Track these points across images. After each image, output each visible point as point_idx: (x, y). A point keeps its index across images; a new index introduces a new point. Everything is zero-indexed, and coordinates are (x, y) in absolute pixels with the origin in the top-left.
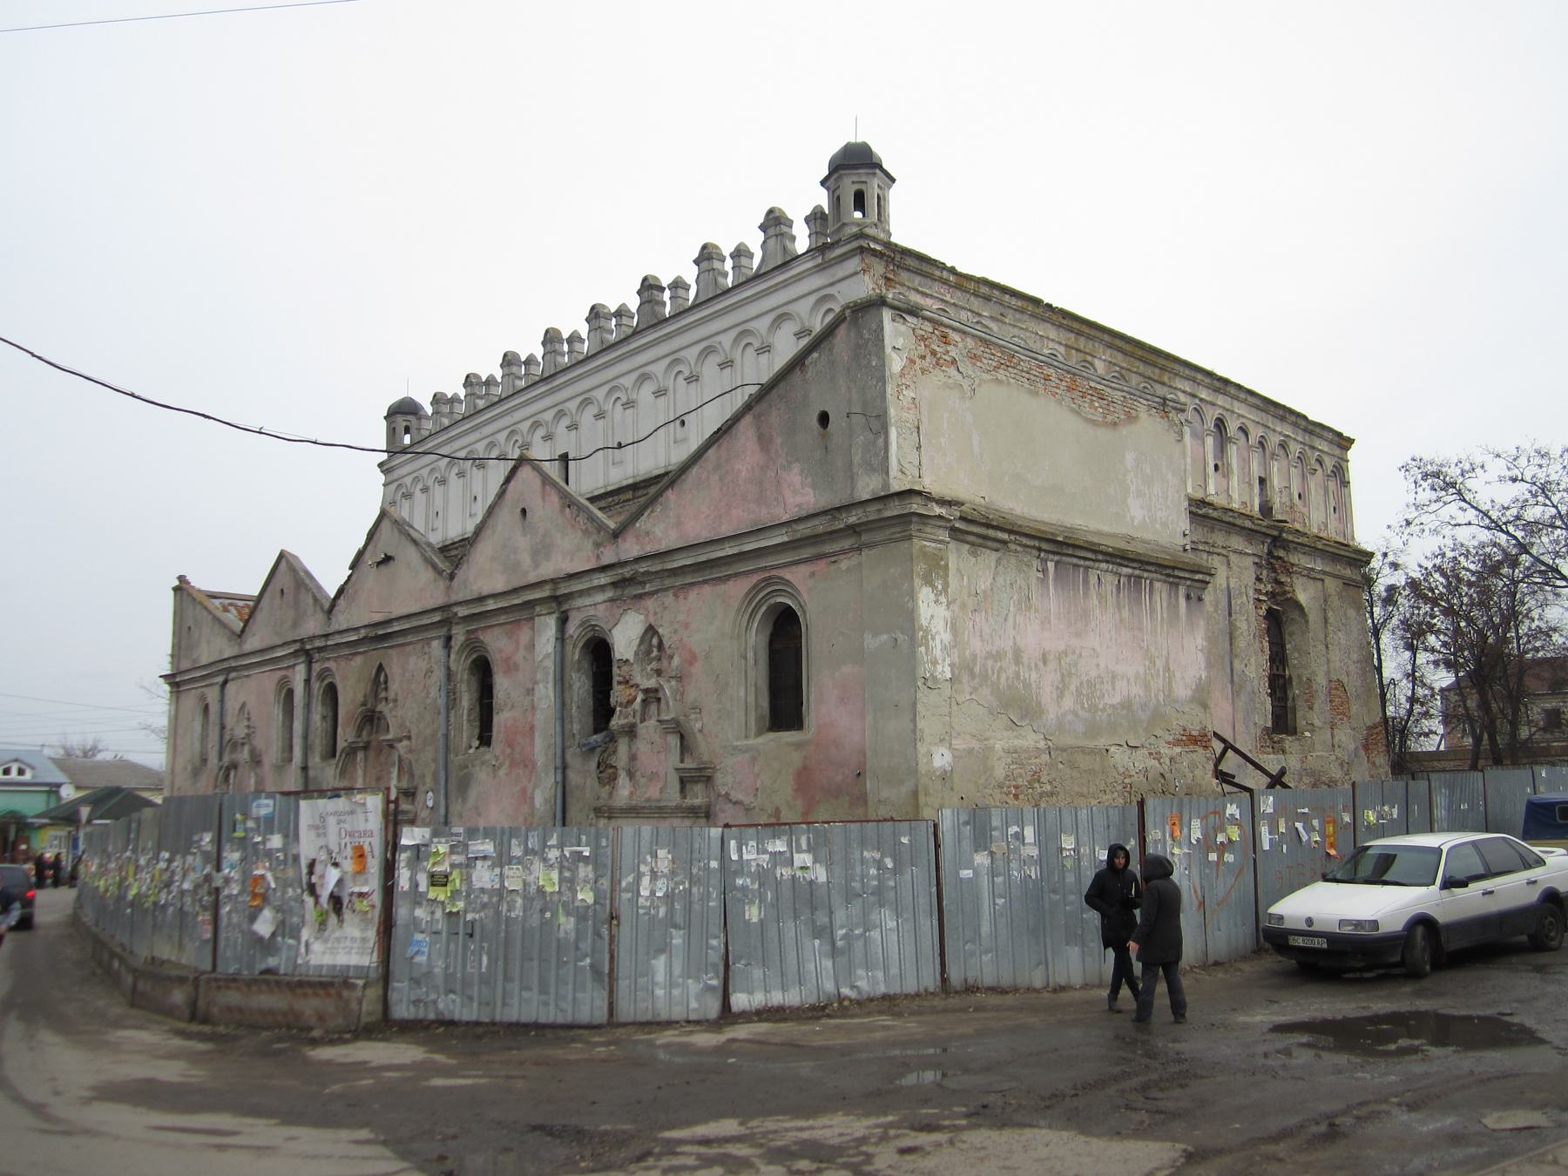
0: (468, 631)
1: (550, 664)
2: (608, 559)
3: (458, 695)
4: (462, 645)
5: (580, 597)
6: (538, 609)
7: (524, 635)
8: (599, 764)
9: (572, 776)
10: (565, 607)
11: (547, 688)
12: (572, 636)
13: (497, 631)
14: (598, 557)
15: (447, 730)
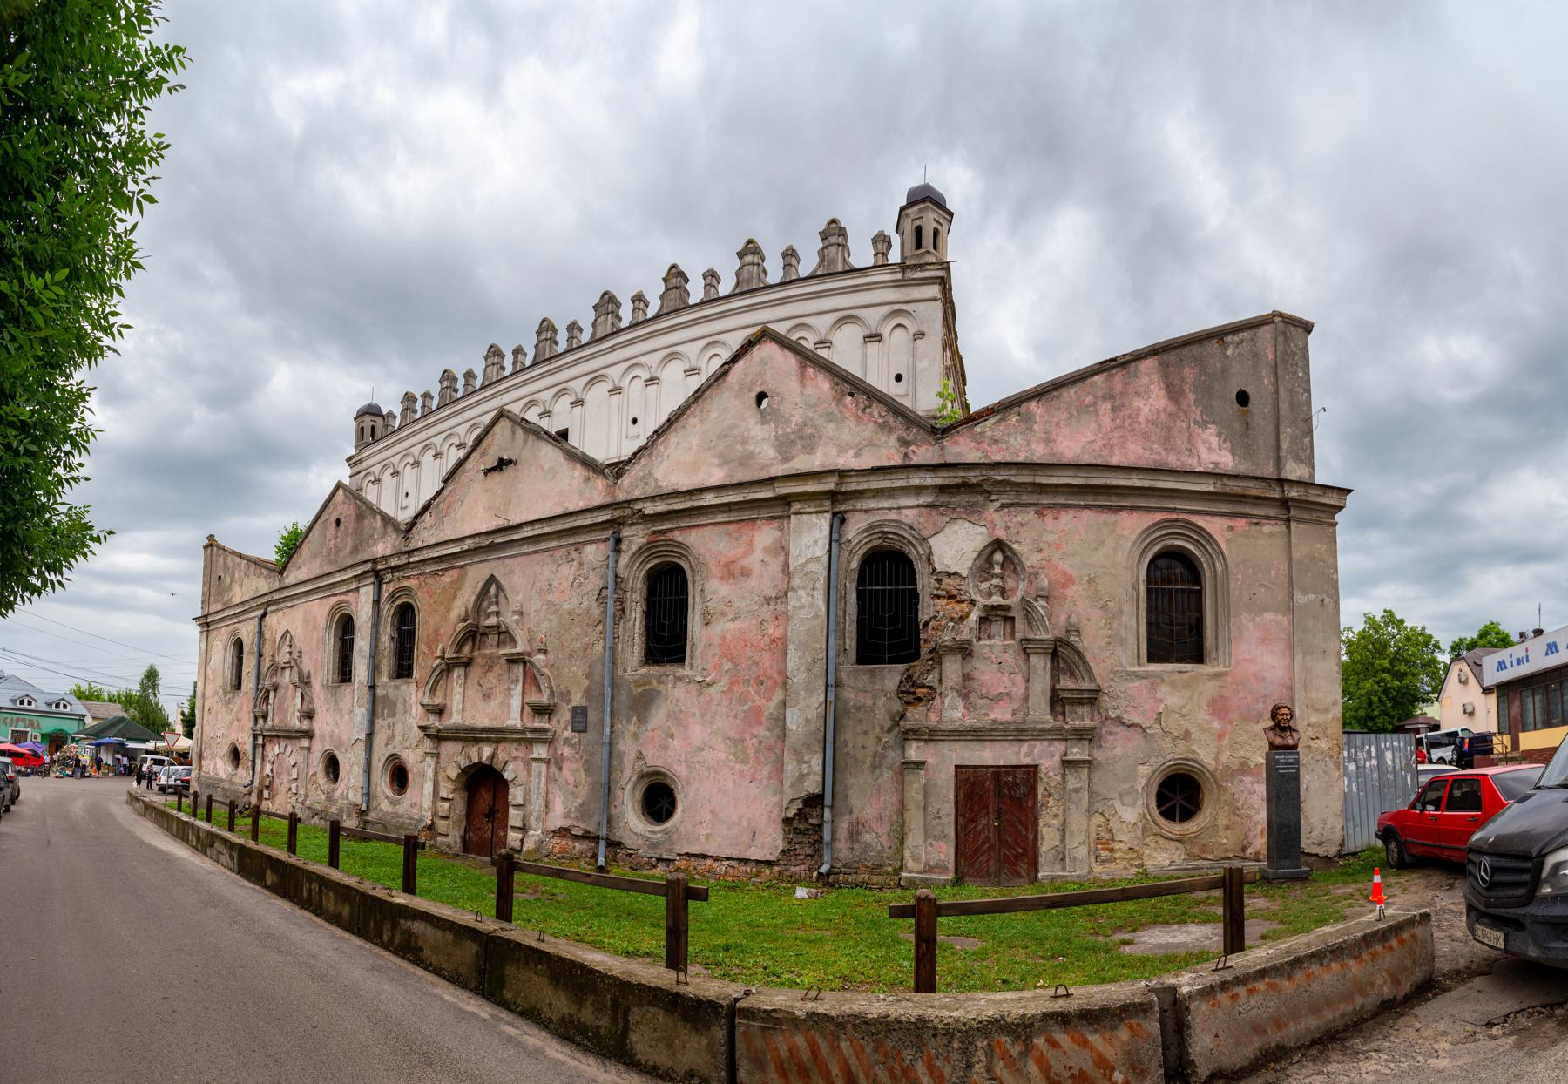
0: (654, 532)
1: (820, 570)
2: (924, 453)
3: (627, 606)
4: (640, 548)
5: (874, 497)
6: (796, 507)
7: (765, 535)
8: (901, 682)
9: (848, 694)
10: (843, 508)
11: (813, 596)
12: (850, 541)
13: (707, 531)
14: (906, 455)
15: (615, 643)
